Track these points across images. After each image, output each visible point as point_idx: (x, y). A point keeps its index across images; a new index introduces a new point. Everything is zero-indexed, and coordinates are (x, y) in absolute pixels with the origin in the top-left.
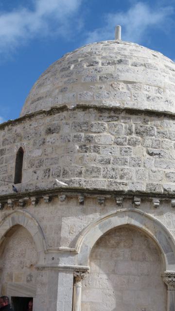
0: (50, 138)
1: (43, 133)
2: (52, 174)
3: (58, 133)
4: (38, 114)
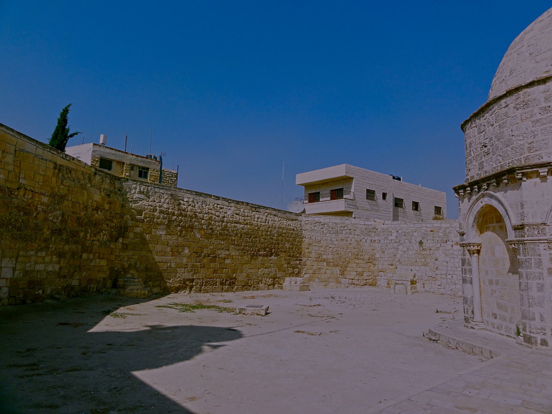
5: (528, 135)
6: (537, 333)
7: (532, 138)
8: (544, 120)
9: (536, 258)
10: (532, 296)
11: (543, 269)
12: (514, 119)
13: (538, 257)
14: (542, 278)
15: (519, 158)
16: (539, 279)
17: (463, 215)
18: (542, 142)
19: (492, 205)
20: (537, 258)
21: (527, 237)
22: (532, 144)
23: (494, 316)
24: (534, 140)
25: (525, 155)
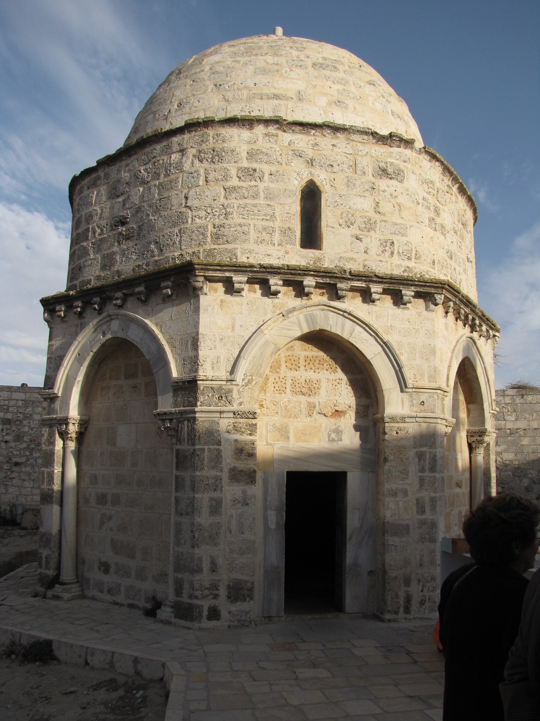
0: (383, 184)
1: (370, 171)
2: (399, 252)
3: (401, 182)
4: (358, 131)
5: (216, 211)
6: (203, 597)
7: (221, 217)
8: (244, 191)
9: (212, 449)
10: (200, 525)
11: (222, 471)
12: (193, 177)
13: (216, 447)
14: (219, 488)
15: (196, 249)
16: (215, 490)
17: (57, 359)
18: (239, 228)
19: (127, 339)
20: (214, 448)
21: (201, 406)
22: (222, 229)
23: (102, 568)
24: (225, 221)
25: (207, 247)
